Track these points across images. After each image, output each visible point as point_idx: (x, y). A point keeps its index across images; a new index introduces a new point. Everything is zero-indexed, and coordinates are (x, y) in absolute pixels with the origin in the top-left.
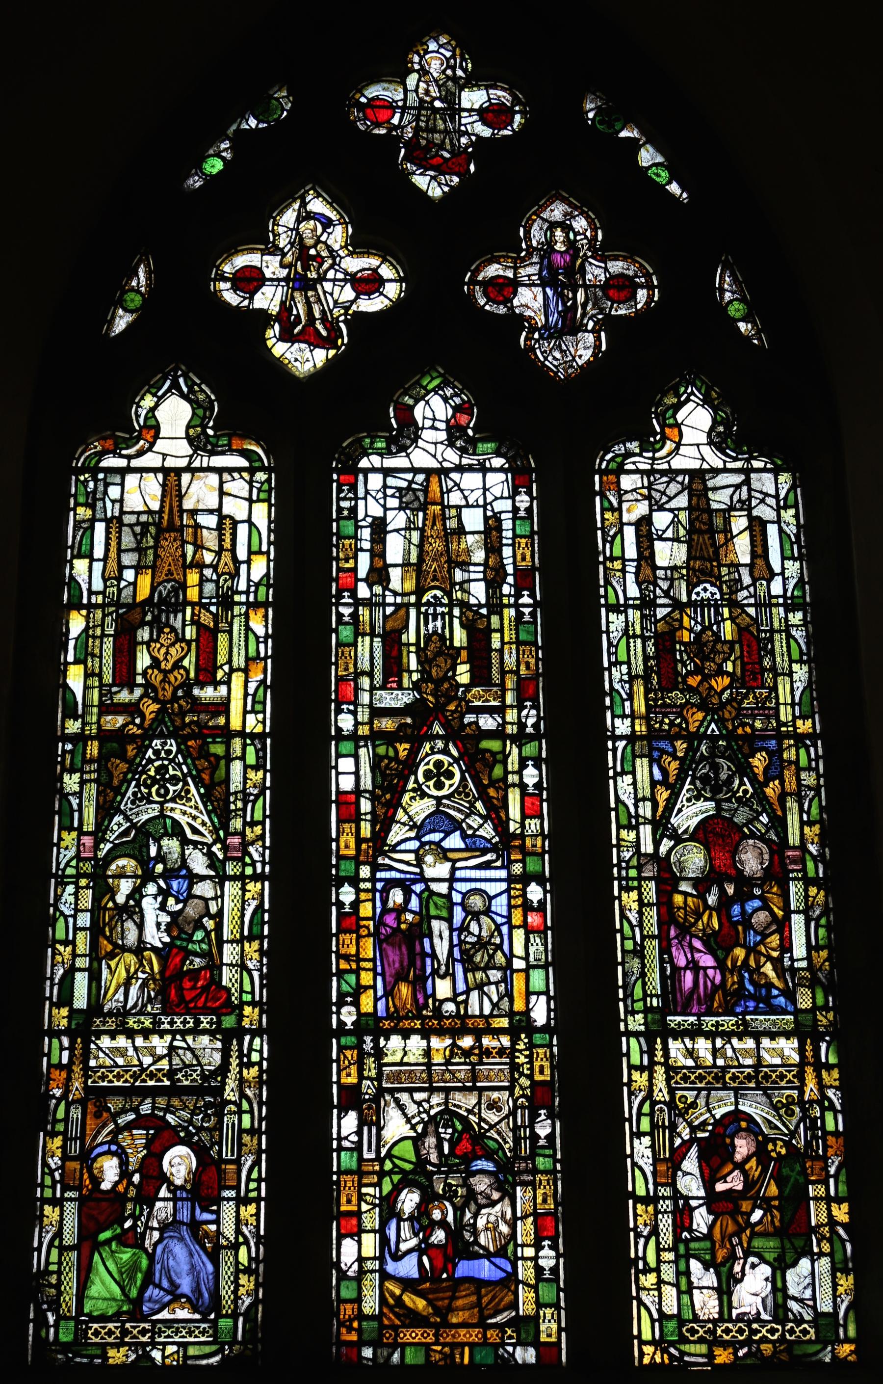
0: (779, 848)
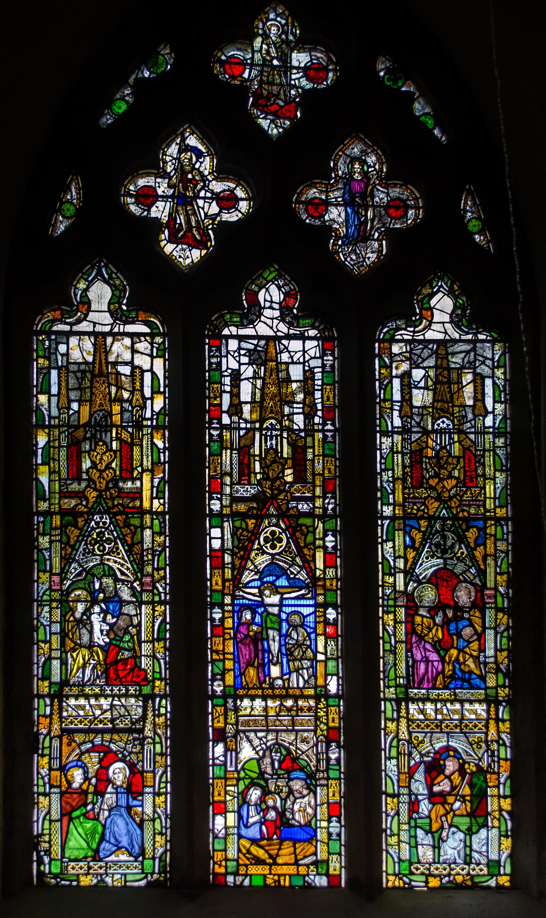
0: (481, 589)
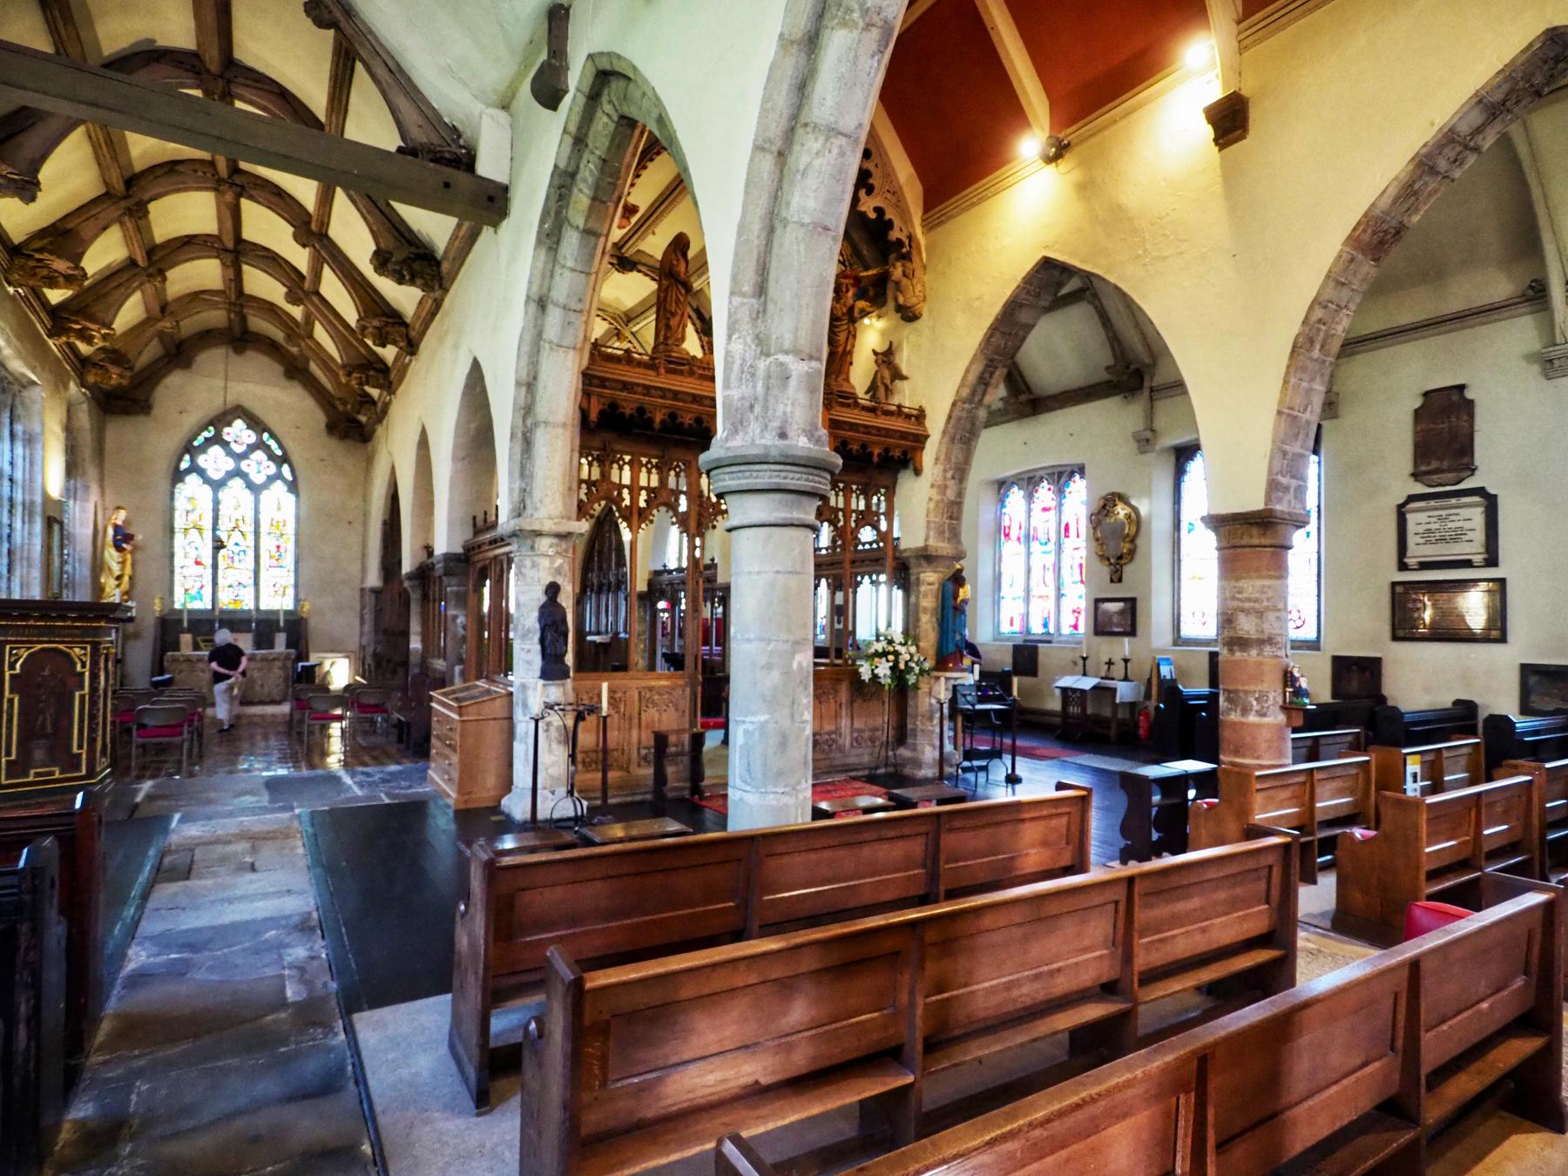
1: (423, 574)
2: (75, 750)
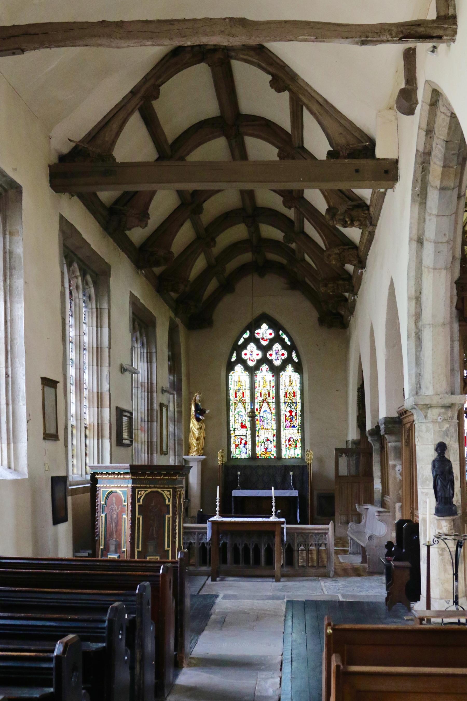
0: (296, 413)
1: (376, 431)
2: (166, 548)
